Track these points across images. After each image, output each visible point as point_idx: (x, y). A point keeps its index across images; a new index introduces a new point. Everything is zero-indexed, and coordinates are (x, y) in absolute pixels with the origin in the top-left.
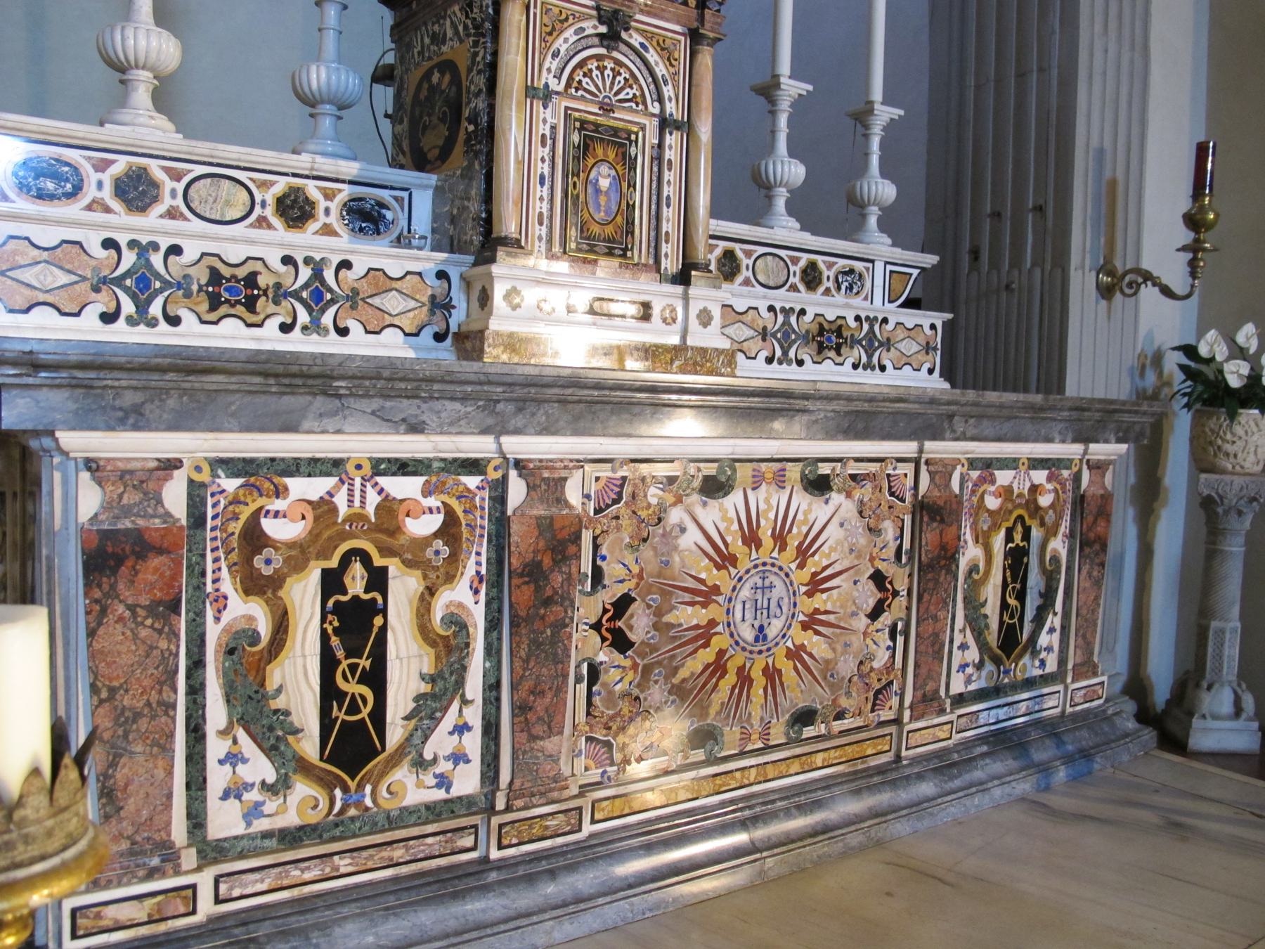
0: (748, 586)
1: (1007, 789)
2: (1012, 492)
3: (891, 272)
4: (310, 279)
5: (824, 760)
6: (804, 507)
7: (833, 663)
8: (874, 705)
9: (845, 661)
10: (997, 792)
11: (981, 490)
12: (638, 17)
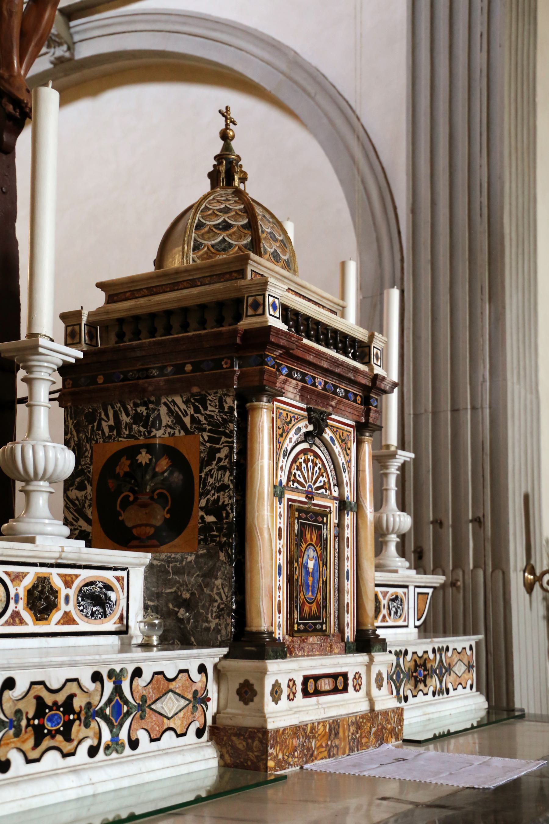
3: (419, 594)
4: (112, 693)
12: (333, 416)
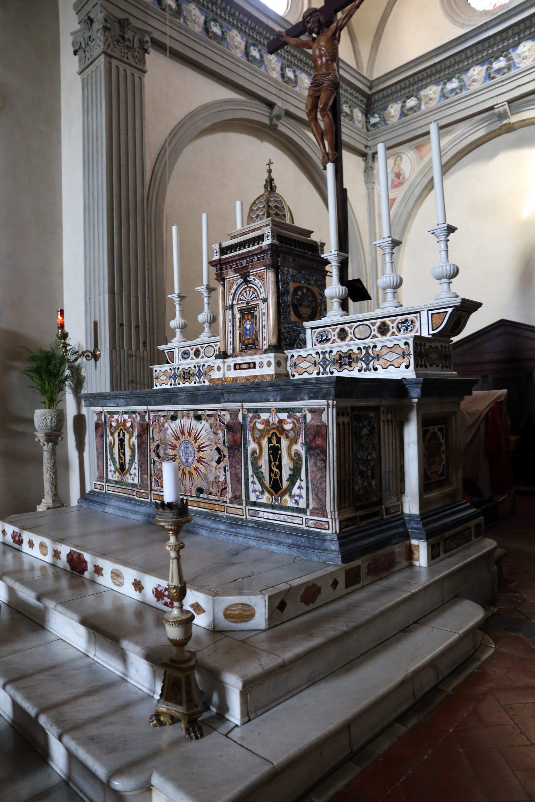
0: (183, 446)
1: (246, 540)
2: (269, 422)
3: (432, 314)
6: (195, 424)
8: (221, 494)
10: (241, 539)
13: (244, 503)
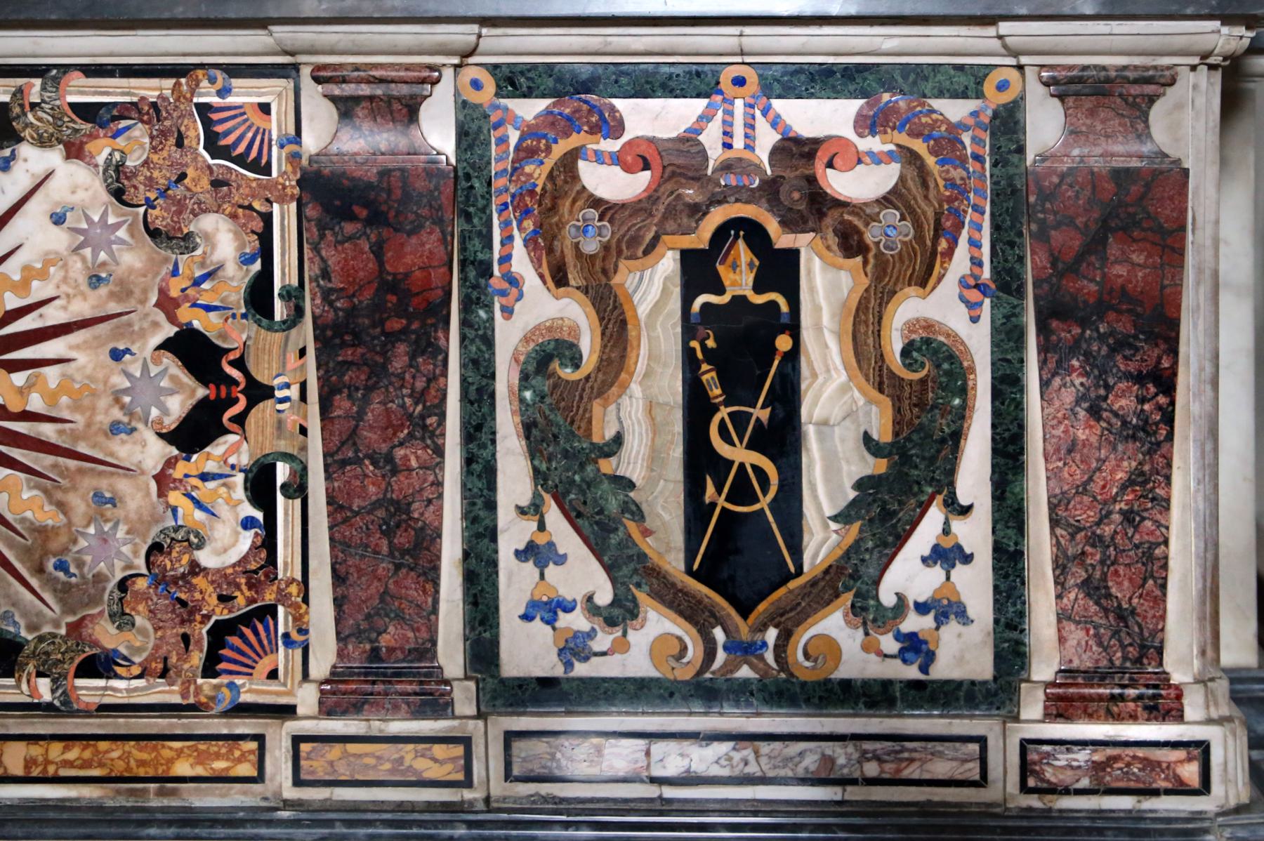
5: (29, 763)
7: (63, 539)
9: (104, 538)
11: (560, 149)
13: (464, 698)
